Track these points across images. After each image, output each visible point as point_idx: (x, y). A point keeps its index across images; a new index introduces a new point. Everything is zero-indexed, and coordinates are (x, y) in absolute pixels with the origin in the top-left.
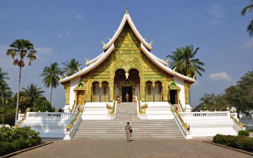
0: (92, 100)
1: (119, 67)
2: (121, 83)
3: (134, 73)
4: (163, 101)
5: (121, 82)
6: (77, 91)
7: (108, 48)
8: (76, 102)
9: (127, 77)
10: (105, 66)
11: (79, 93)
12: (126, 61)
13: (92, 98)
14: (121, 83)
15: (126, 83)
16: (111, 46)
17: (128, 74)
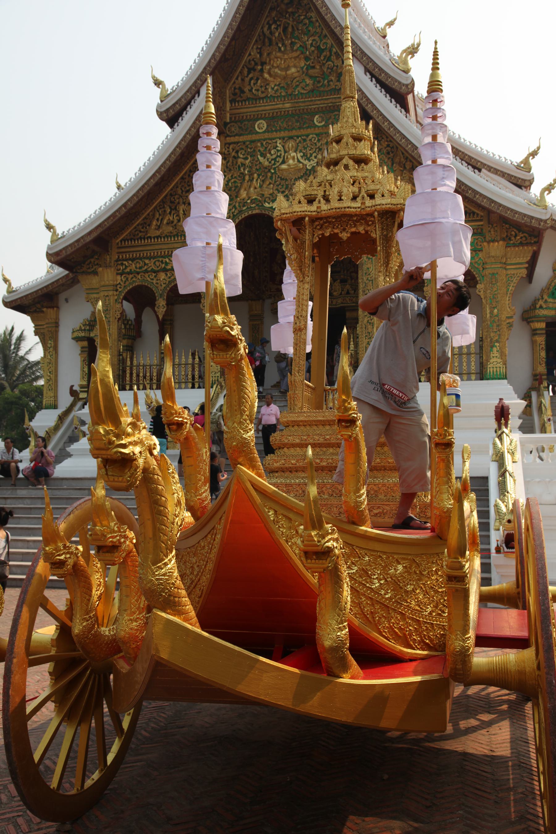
1: (250, 208)
6: (85, 343)
13: (124, 371)
16: (198, 92)
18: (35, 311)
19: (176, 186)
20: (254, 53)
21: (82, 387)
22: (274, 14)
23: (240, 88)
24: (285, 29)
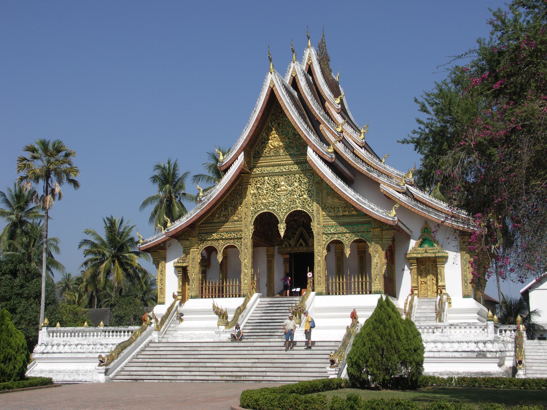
0: (202, 293)
2: (286, 246)
3: (300, 222)
4: (370, 293)
5: (286, 243)
7: (231, 165)
8: (180, 297)
9: (282, 234)
10: (230, 208)
11: (183, 273)
12: (278, 193)
14: (286, 246)
15: (298, 245)
16: (237, 158)
17: (285, 225)
18: (154, 251)
19: (227, 198)
20: (264, 135)
21: (178, 293)
22: (273, 117)
23: (258, 151)
24: (279, 124)
